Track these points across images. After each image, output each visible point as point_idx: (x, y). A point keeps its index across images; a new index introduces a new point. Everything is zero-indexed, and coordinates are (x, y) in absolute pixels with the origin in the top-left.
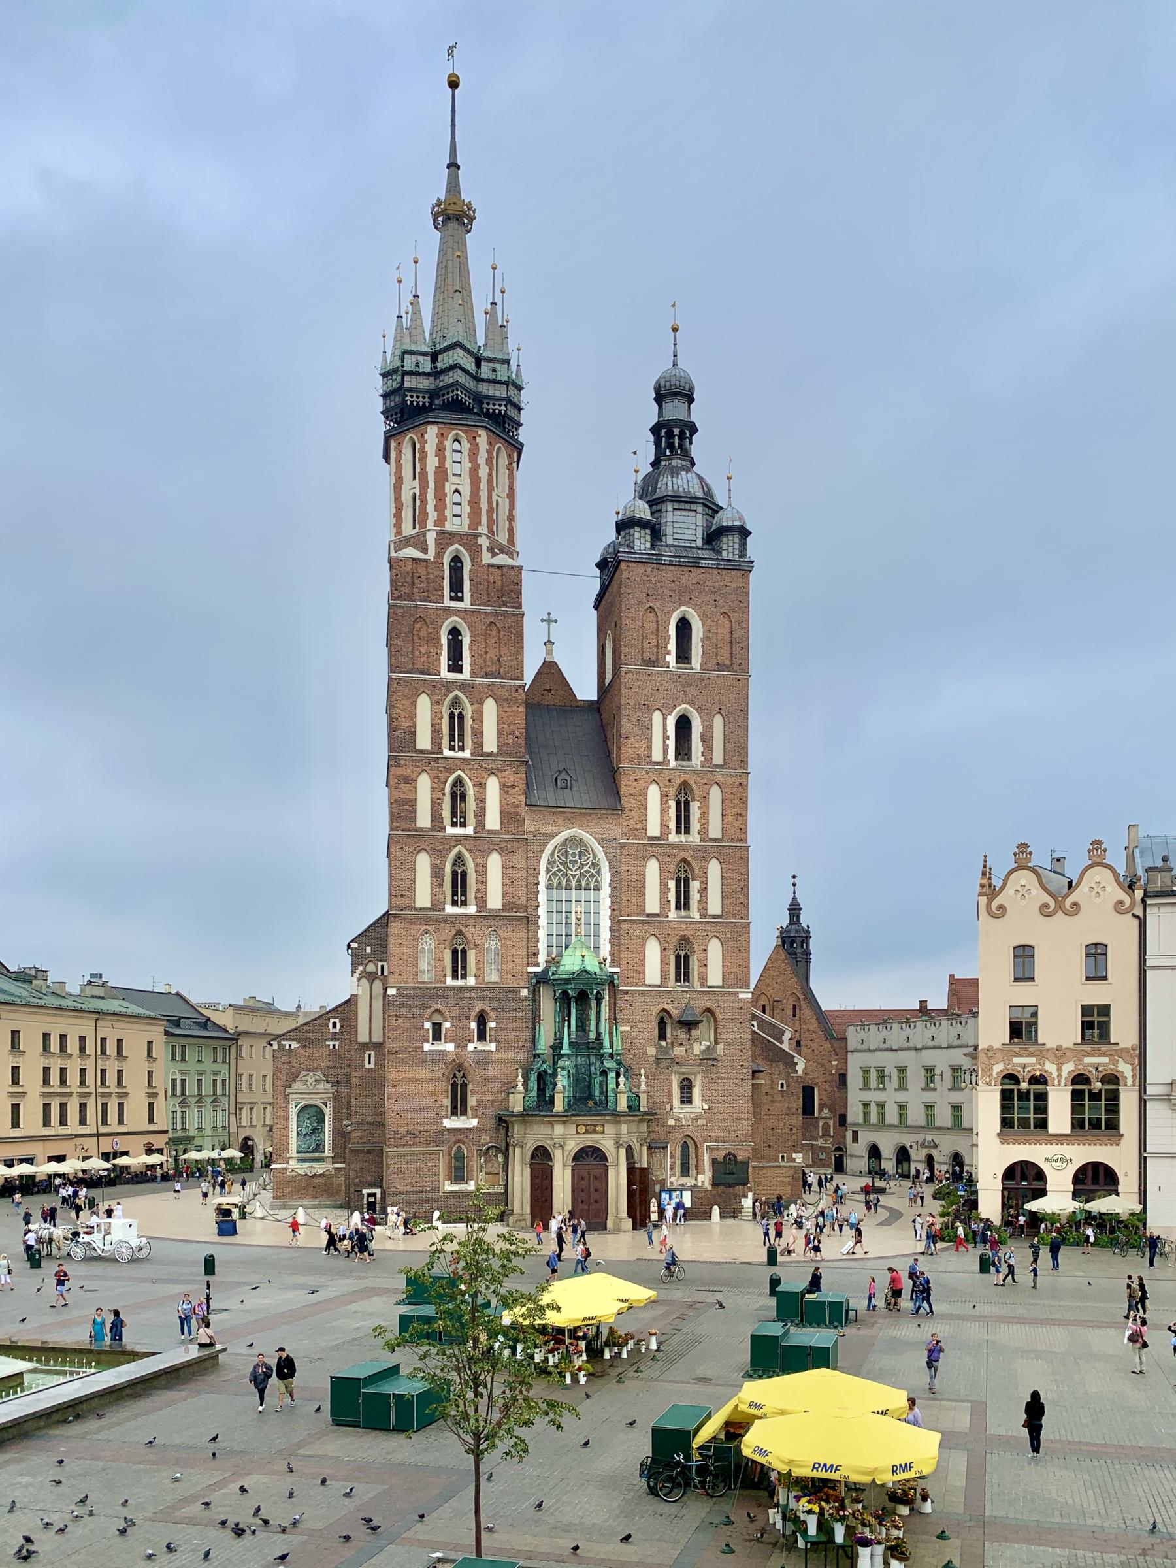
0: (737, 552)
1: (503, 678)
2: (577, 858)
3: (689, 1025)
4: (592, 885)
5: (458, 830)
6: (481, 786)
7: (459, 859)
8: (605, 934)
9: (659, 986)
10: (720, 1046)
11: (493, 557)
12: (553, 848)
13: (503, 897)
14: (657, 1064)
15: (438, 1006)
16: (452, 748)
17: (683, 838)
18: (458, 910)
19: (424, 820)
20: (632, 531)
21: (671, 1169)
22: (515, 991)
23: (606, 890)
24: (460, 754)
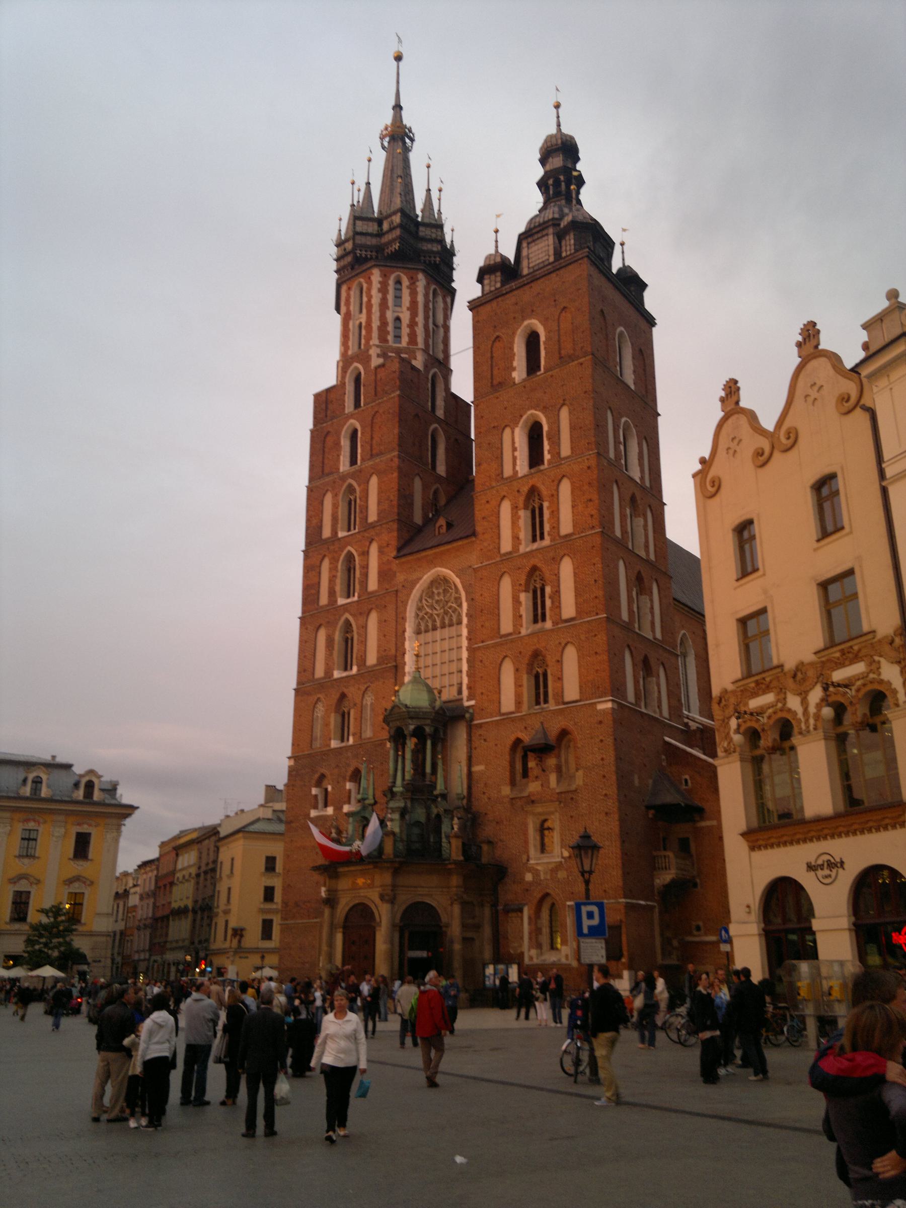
0: (573, 247)
2: (442, 597)
4: (454, 619)
5: (349, 601)
6: (365, 554)
7: (348, 625)
8: (465, 667)
10: (580, 773)
12: (418, 595)
13: (378, 652)
14: (512, 804)
16: (349, 530)
17: (535, 546)
18: (345, 674)
19: (324, 600)
21: (530, 939)
22: (382, 744)
23: (465, 620)
24: (353, 532)
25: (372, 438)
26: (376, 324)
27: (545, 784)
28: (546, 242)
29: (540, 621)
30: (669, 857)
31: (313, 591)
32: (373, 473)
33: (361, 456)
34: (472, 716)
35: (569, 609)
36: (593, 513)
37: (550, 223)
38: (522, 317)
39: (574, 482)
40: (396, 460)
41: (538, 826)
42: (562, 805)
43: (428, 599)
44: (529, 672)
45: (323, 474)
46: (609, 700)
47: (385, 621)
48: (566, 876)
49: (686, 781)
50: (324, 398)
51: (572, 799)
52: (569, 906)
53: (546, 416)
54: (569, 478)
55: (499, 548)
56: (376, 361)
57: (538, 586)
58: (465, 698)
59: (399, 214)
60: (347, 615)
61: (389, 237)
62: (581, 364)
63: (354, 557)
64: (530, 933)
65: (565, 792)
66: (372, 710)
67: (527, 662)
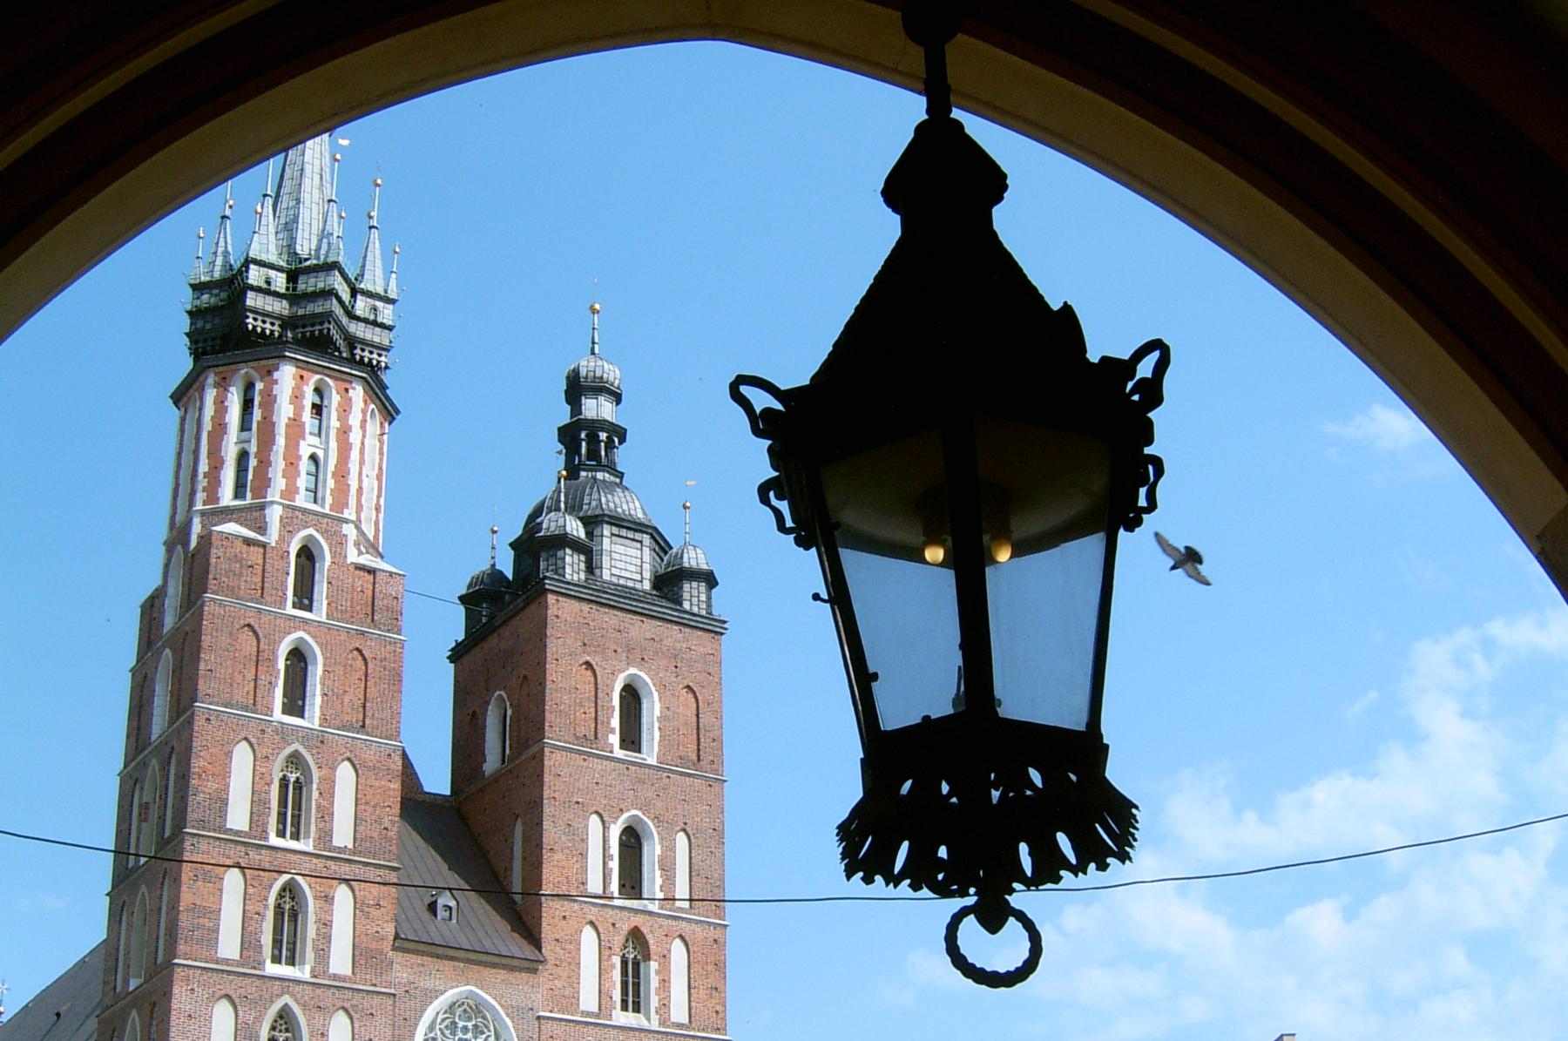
0: (704, 606)
11: (359, 556)
20: (560, 553)
28: (639, 552)
36: (718, 1008)
37: (650, 531)
53: (659, 833)
54: (687, 945)
56: (353, 556)
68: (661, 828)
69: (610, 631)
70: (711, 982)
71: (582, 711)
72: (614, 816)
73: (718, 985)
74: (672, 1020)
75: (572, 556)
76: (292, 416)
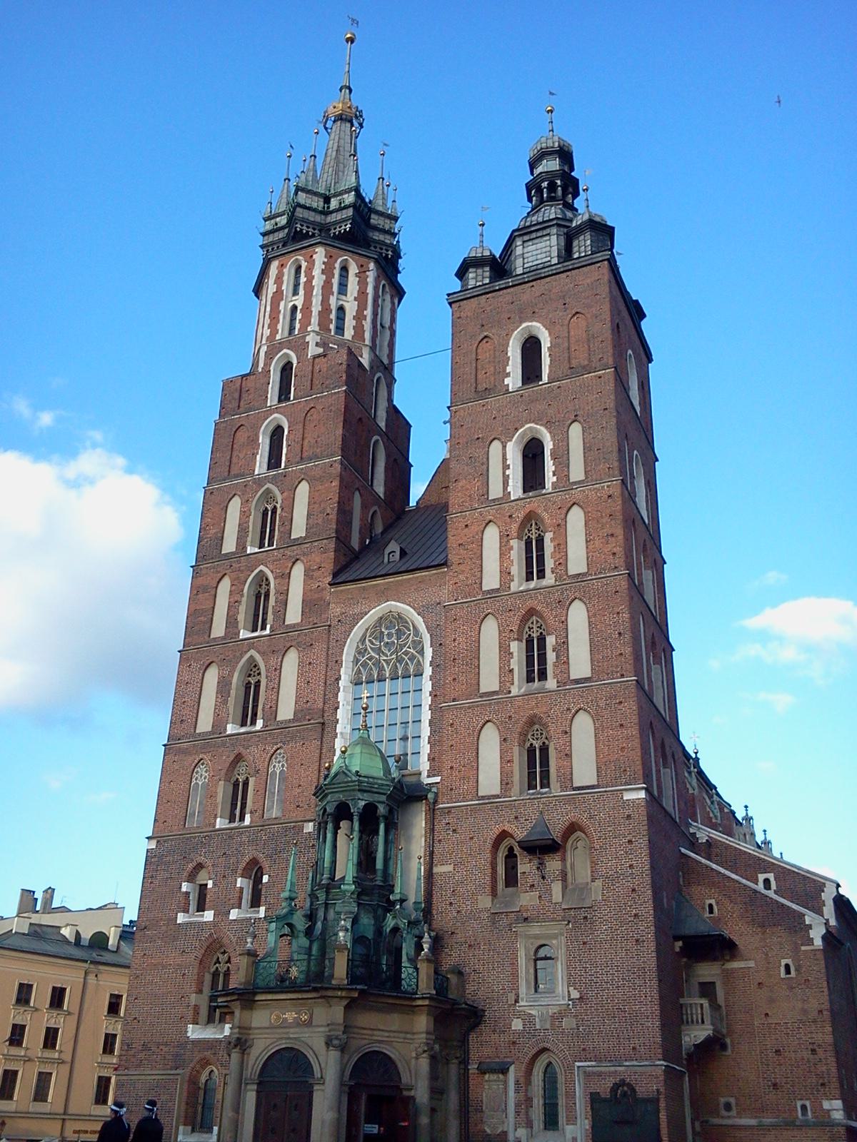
0: (590, 248)
1: (318, 458)
2: (394, 639)
3: (543, 848)
6: (285, 577)
7: (253, 667)
8: (426, 731)
9: (497, 797)
10: (598, 883)
15: (201, 859)
17: (532, 584)
18: (243, 730)
19: (218, 630)
20: (467, 275)
21: (517, 1113)
23: (428, 671)
25: (303, 439)
26: (316, 308)
27: (545, 895)
28: (548, 242)
29: (536, 680)
30: (702, 1005)
31: (202, 618)
32: (303, 479)
33: (286, 458)
34: (436, 794)
35: (580, 665)
36: (615, 550)
37: (555, 222)
38: (520, 317)
39: (589, 512)
40: (338, 467)
41: (532, 953)
42: (570, 926)
43: (374, 641)
44: (521, 745)
45: (229, 476)
46: (643, 788)
47: (310, 663)
48: (575, 1026)
49: (711, 906)
50: (239, 384)
51: (585, 918)
52: (579, 1067)
53: (550, 433)
54: (582, 508)
55: (481, 583)
56: (313, 350)
57: (535, 635)
58: (425, 774)
59: (353, 193)
60: (252, 652)
61: (339, 216)
62: (600, 377)
63: (267, 579)
64: (517, 1105)
65: (575, 909)
66: (283, 778)
67: (519, 730)
68: (553, 428)
69: (504, 306)
70: (607, 530)
71: (483, 372)
72: (510, 435)
73: (614, 532)
74: (569, 574)
75: (476, 272)
76: (275, 290)
